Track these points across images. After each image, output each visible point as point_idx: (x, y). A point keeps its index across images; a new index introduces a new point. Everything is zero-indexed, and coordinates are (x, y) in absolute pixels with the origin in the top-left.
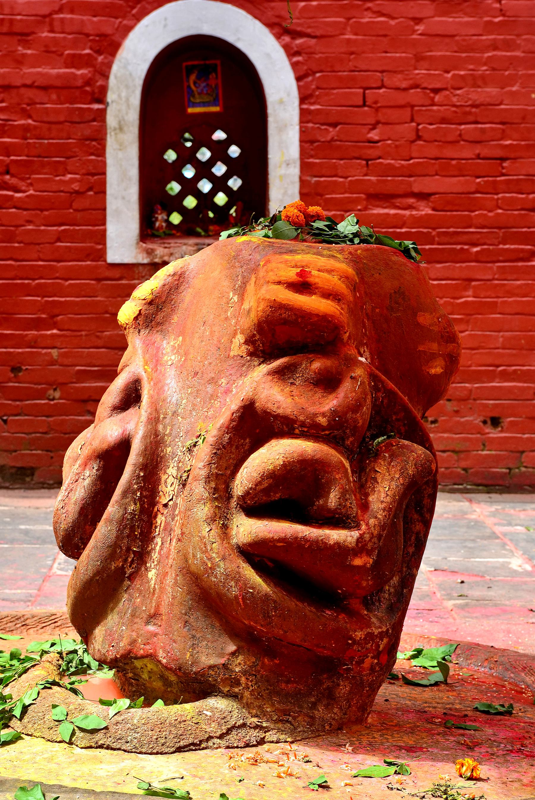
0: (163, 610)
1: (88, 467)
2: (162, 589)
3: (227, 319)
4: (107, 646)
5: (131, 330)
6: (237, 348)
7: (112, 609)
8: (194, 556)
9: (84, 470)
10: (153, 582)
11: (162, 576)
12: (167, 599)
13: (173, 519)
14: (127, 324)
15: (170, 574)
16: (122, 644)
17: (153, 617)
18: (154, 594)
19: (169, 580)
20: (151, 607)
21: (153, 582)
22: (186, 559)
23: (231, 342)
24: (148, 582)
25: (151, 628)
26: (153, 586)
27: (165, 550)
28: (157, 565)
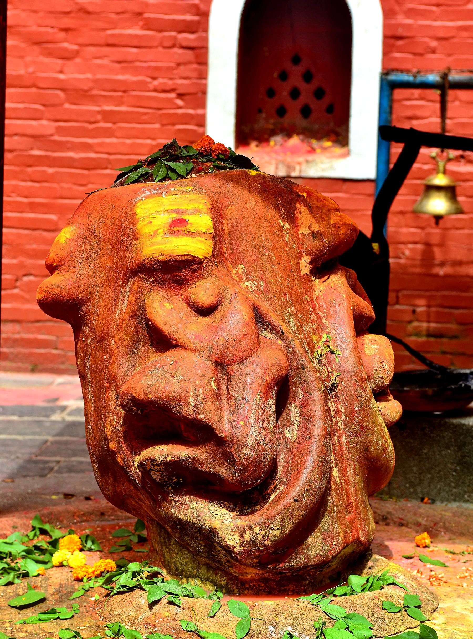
0: (352, 498)
1: (268, 396)
2: (347, 483)
3: (286, 244)
4: (329, 547)
5: (211, 264)
6: (304, 268)
7: (323, 515)
8: (377, 442)
9: (267, 399)
10: (338, 479)
11: (343, 471)
12: (352, 488)
13: (332, 421)
14: (206, 258)
15: (348, 467)
16: (340, 539)
17: (348, 506)
18: (342, 488)
19: (350, 472)
20: (344, 499)
21: (338, 479)
22: (366, 448)
23: (299, 263)
24: (335, 480)
25: (349, 516)
26: (339, 482)
27: (337, 449)
28: (335, 463)
